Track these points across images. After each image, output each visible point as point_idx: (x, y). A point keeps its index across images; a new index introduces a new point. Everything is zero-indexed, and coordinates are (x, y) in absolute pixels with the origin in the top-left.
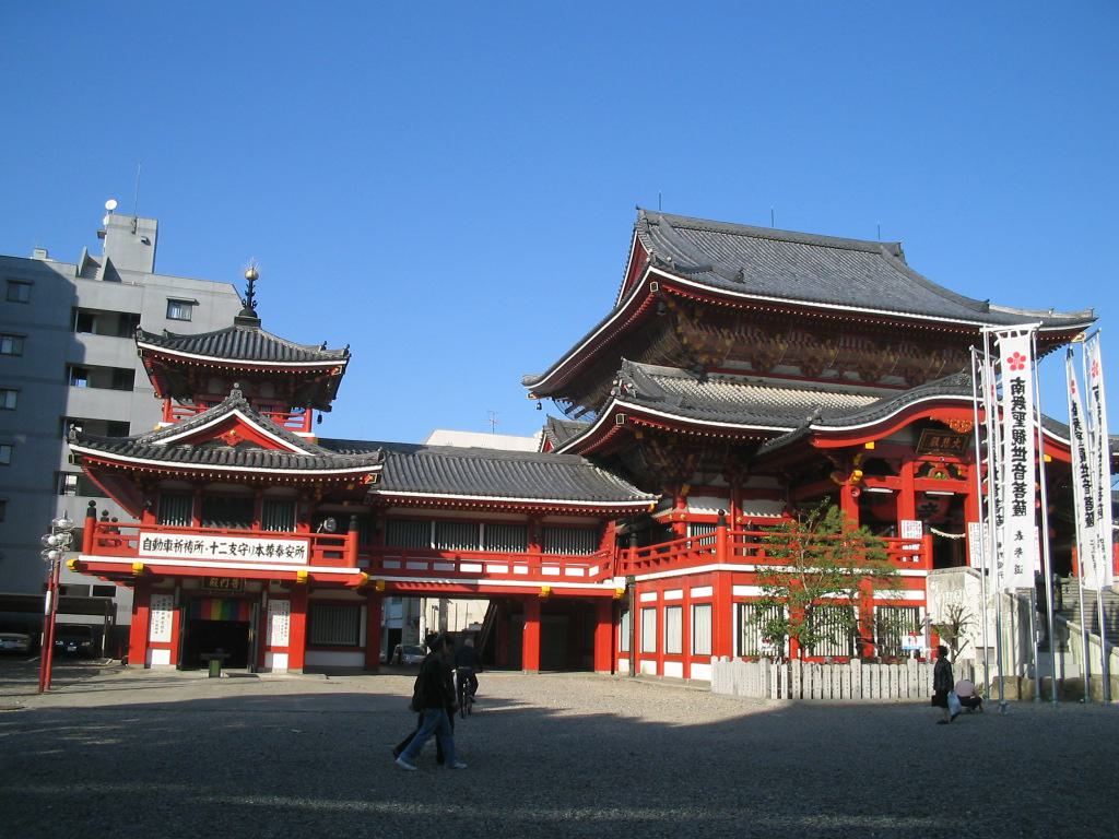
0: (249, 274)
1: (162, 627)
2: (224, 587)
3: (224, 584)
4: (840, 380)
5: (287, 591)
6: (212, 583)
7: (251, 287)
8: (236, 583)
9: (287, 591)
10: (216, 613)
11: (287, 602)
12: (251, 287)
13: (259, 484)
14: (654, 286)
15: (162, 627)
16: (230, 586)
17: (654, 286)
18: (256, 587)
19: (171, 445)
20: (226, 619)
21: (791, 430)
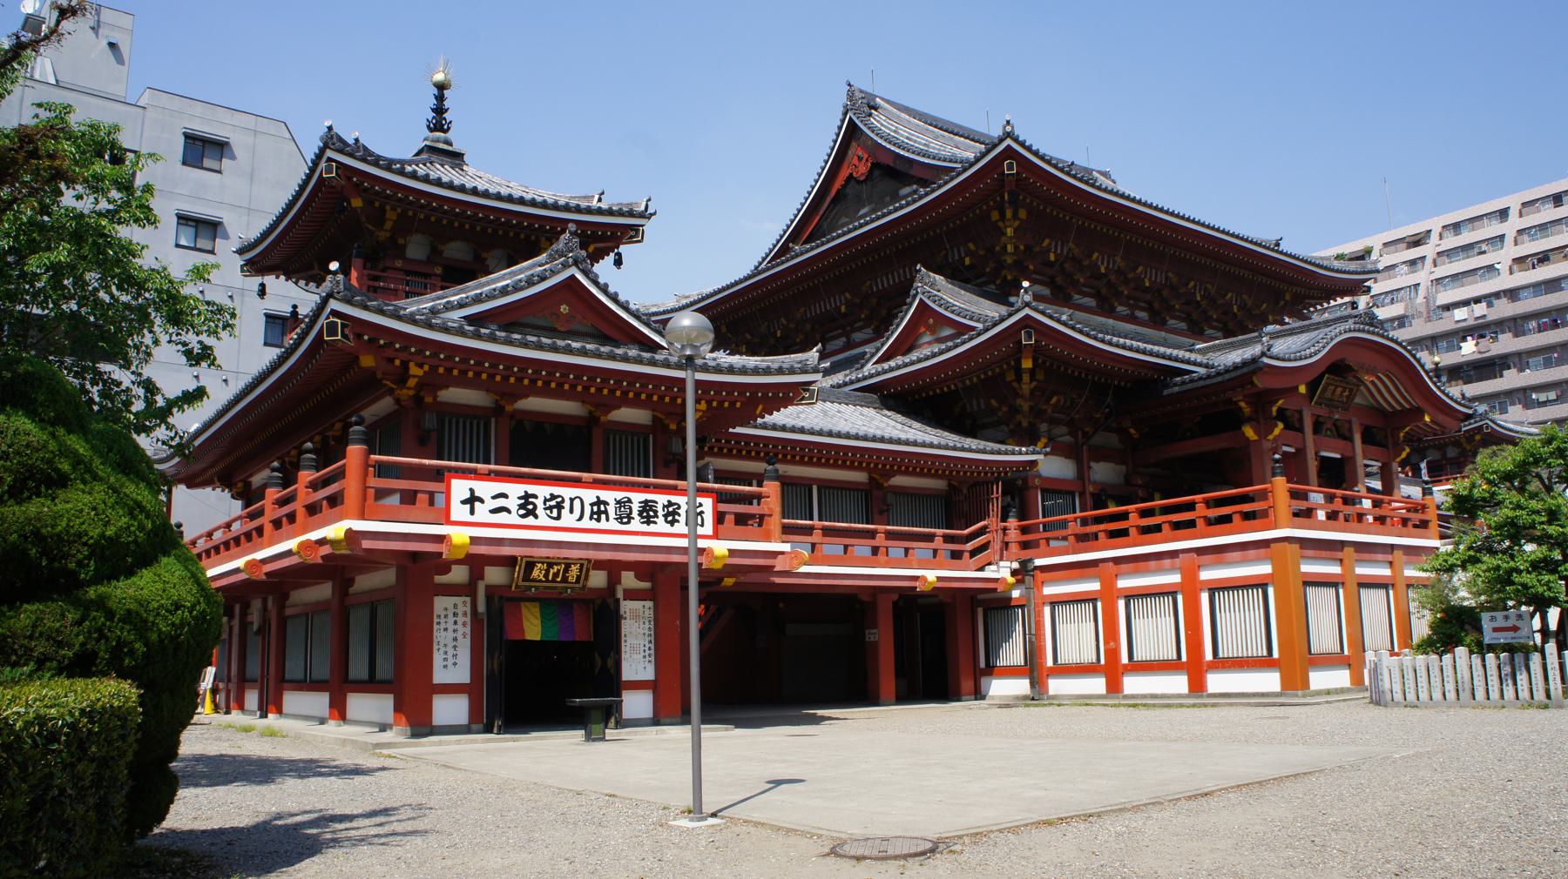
0: (439, 77)
1: (455, 656)
2: (554, 581)
3: (556, 575)
4: (1132, 319)
5: (646, 585)
6: (535, 573)
7: (440, 98)
8: (574, 570)
9: (646, 585)
10: (533, 629)
11: (649, 604)
12: (440, 98)
13: (603, 390)
14: (1010, 167)
15: (455, 656)
16: (565, 580)
17: (1010, 167)
18: (598, 579)
19: (470, 319)
20: (553, 636)
21: (1202, 371)
